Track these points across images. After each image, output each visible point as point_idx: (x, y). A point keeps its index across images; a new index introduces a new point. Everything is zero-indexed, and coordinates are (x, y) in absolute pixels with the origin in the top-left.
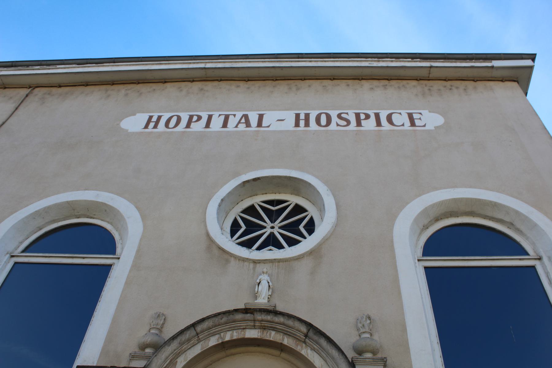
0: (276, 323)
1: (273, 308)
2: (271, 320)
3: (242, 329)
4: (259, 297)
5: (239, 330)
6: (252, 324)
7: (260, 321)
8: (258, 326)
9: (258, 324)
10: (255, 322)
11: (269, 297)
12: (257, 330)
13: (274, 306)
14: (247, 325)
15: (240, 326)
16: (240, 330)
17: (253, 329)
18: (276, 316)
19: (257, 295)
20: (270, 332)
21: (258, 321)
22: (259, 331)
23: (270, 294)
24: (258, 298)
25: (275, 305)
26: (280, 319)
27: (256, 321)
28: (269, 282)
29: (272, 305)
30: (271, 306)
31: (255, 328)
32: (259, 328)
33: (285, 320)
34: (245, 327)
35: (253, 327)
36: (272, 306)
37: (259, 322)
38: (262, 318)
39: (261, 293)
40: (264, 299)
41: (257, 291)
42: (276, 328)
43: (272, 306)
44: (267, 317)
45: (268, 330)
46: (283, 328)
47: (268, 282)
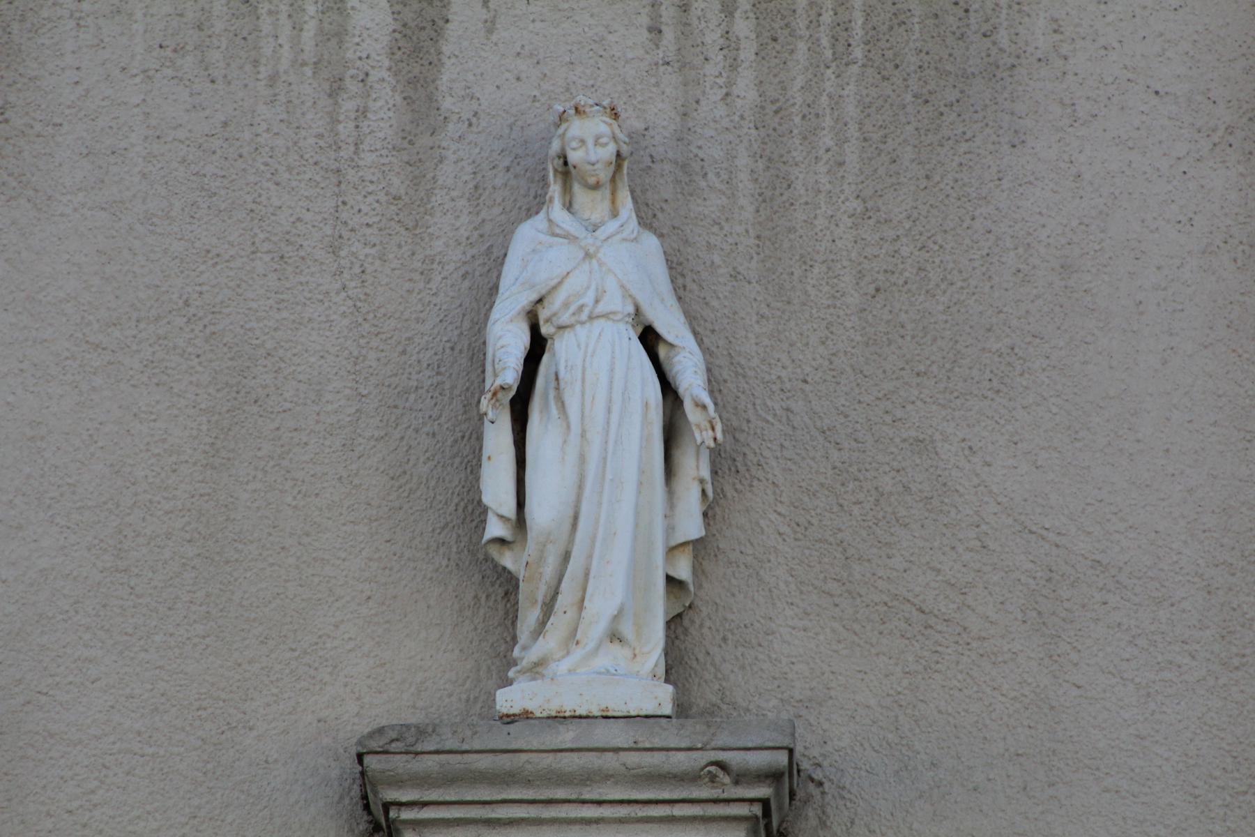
1: (763, 791)
4: (548, 608)
11: (683, 571)
13: (774, 776)
19: (507, 560)
23: (692, 527)
24: (529, 617)
25: (782, 759)
28: (671, 325)
30: (722, 766)
36: (740, 778)
39: (566, 557)
40: (615, 636)
41: (509, 509)
43: (740, 778)
47: (649, 338)
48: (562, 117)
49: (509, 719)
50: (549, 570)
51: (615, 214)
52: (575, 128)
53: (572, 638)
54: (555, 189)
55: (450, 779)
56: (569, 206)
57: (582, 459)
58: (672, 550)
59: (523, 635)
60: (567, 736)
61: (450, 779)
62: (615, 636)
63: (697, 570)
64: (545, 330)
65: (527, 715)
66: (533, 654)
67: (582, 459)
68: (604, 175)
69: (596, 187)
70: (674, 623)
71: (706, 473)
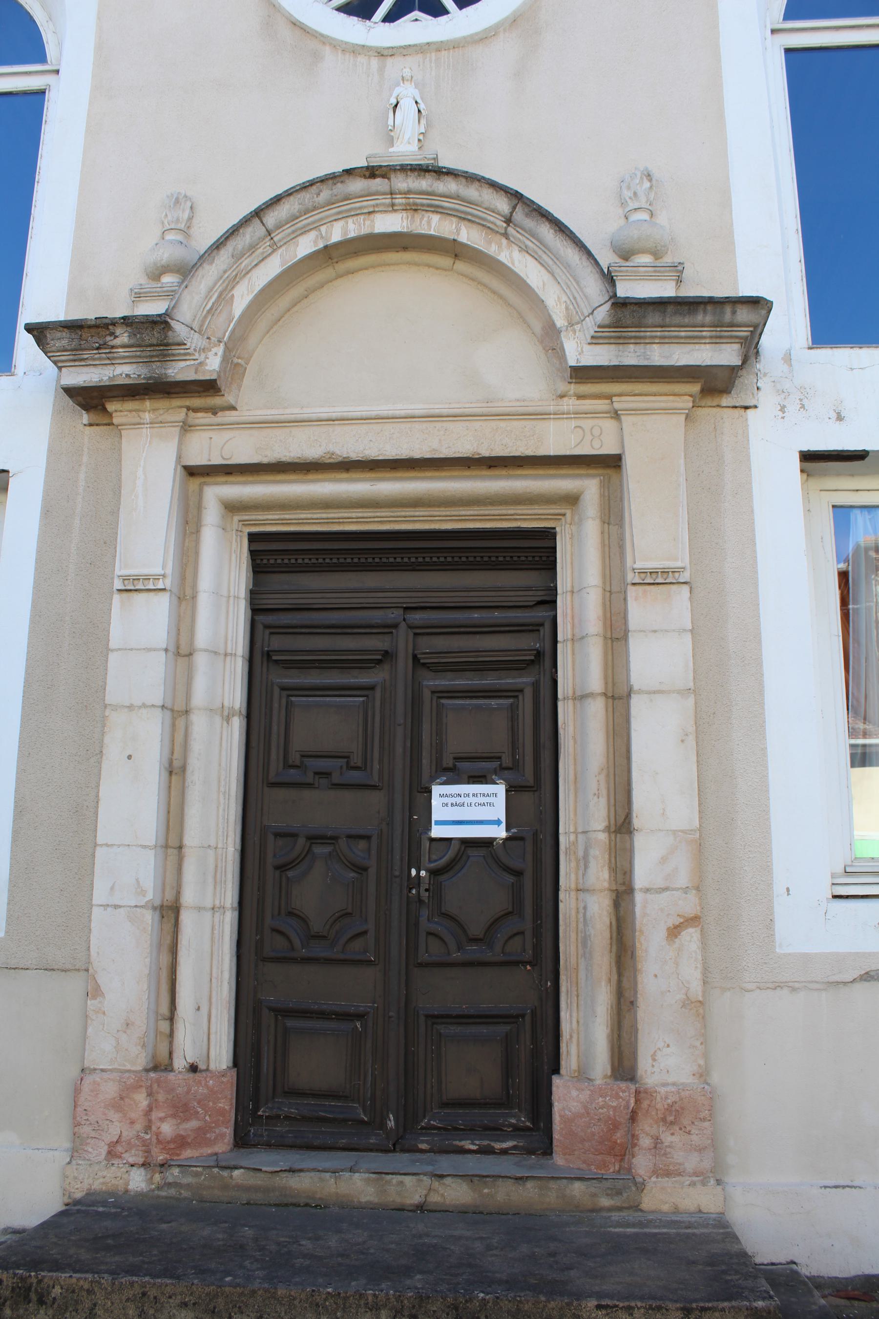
6: (388, 201)
7: (405, 194)
8: (400, 205)
10: (394, 196)
12: (401, 215)
21: (400, 194)
22: (405, 215)
27: (396, 194)
31: (395, 211)
32: (403, 210)
35: (391, 209)
37: (403, 196)
45: (424, 213)
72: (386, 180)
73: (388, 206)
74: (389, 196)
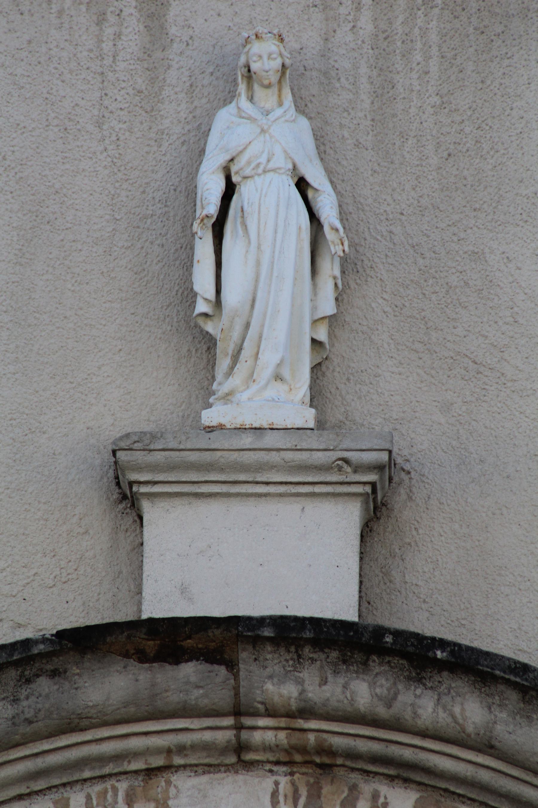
0: (424, 734)
1: (372, 477)
2: (382, 711)
3: (136, 772)
4: (236, 358)
5: (108, 784)
6: (228, 736)
7: (290, 715)
8: (267, 748)
9: (269, 736)
10: (248, 721)
11: (322, 335)
12: (268, 783)
13: (379, 468)
14: (181, 749)
15: (118, 757)
16: (123, 786)
17: (228, 768)
18: (419, 680)
20: (375, 796)
21: (271, 713)
22: (284, 781)
25: (385, 456)
26: (457, 710)
27: (256, 714)
29: (352, 456)
30: (346, 461)
31: (249, 765)
32: (277, 763)
33: (504, 715)
34: (159, 761)
35: (233, 759)
36: (357, 468)
37: (283, 722)
38: (302, 692)
39: (247, 325)
40: (278, 377)
42: (428, 771)
43: (357, 468)
44: (345, 687)
45: (355, 777)
46: (485, 776)
48: (247, 41)
49: (210, 429)
50: (236, 335)
51: (280, 104)
52: (256, 48)
53: (251, 378)
54: (242, 87)
55: (172, 467)
56: (251, 99)
57: (258, 263)
58: (315, 322)
59: (219, 375)
60: (247, 441)
61: (172, 467)
62: (278, 377)
63: (331, 334)
64: (235, 179)
65: (221, 427)
66: (226, 388)
67: (258, 263)
68: (274, 78)
69: (269, 86)
70: (316, 368)
71: (337, 272)
72: (222, 670)
73: (224, 750)
74: (229, 721)
